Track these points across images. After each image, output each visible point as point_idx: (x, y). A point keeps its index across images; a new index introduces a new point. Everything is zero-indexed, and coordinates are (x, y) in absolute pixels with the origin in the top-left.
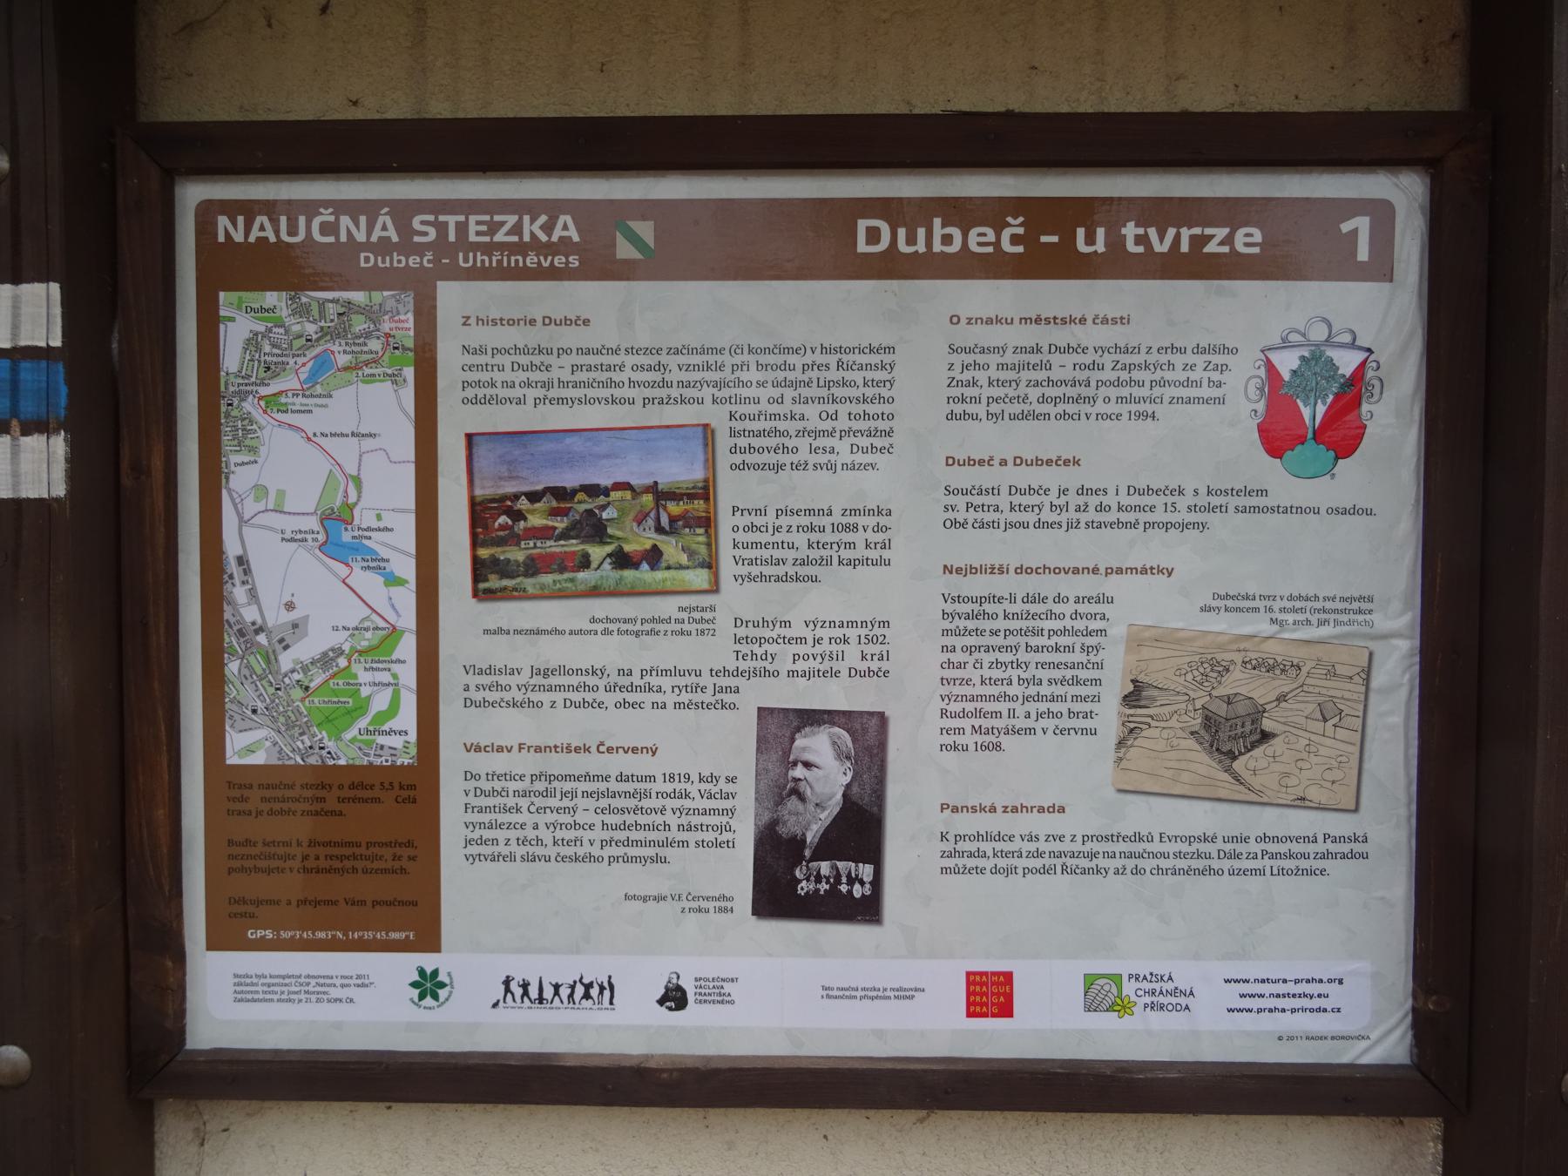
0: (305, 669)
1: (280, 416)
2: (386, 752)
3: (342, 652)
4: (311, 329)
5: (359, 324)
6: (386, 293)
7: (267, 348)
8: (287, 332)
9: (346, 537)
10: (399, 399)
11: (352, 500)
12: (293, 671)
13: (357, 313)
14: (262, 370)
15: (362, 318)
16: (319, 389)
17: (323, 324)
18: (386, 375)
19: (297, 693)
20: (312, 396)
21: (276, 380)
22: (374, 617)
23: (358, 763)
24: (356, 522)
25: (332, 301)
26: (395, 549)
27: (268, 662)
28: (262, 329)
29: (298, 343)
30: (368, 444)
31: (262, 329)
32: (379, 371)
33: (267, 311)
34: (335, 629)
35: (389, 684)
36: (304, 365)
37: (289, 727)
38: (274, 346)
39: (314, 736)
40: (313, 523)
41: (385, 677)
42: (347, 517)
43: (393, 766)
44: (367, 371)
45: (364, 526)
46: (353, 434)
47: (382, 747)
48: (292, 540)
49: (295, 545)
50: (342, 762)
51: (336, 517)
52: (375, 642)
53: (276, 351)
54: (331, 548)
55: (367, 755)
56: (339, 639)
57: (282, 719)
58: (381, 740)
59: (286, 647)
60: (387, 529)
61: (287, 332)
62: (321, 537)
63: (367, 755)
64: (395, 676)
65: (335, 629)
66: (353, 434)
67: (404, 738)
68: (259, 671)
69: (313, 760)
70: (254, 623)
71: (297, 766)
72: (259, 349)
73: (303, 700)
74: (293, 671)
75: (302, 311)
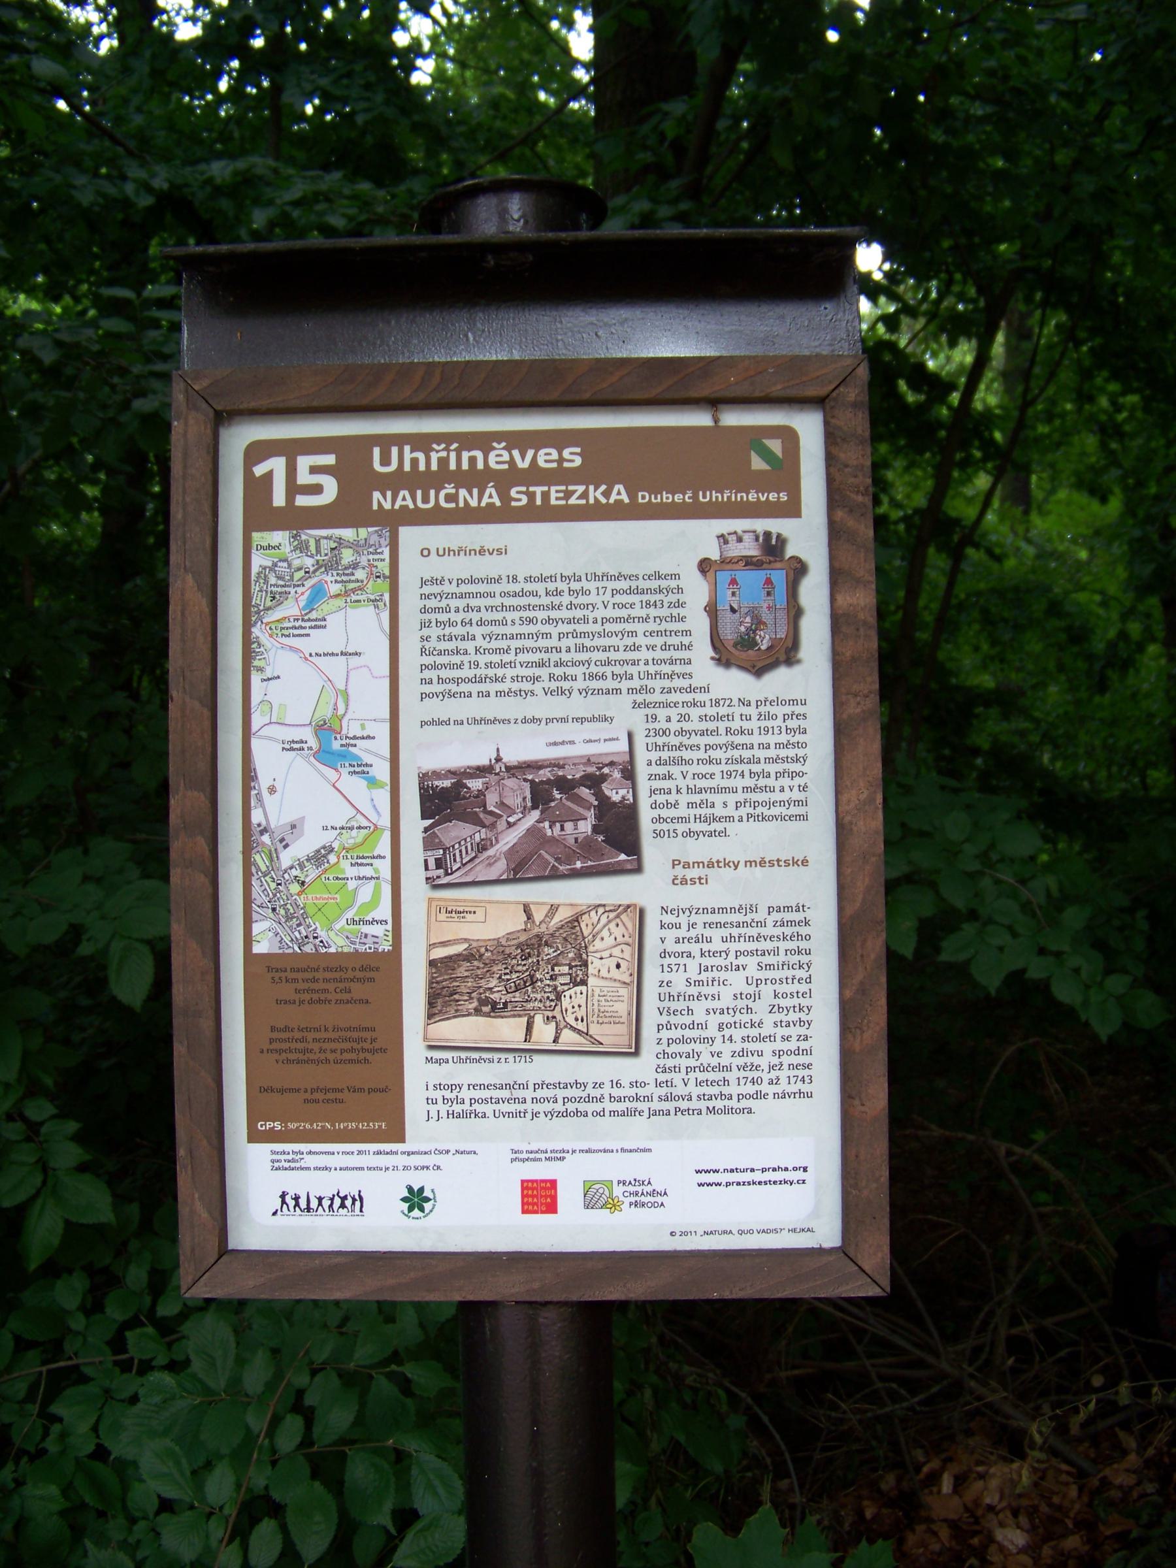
0: (302, 866)
1: (284, 640)
2: (370, 940)
3: (332, 850)
4: (309, 562)
5: (347, 556)
6: (370, 529)
7: (273, 580)
8: (290, 566)
9: (336, 745)
10: (379, 620)
11: (341, 712)
12: (291, 868)
13: (347, 547)
14: (269, 599)
15: (350, 551)
16: (314, 615)
17: (318, 558)
18: (369, 600)
19: (295, 888)
20: (309, 620)
21: (279, 608)
22: (359, 816)
23: (346, 950)
24: (344, 732)
25: (326, 538)
26: (376, 755)
27: (271, 860)
28: (270, 564)
29: (298, 575)
30: (354, 661)
31: (270, 564)
32: (364, 597)
33: (274, 548)
34: (325, 828)
35: (372, 878)
36: (303, 594)
37: (289, 918)
38: (279, 578)
39: (309, 926)
40: (308, 735)
41: (367, 871)
42: (337, 727)
43: (376, 952)
44: (354, 598)
45: (351, 735)
46: (342, 653)
47: (366, 936)
48: (292, 749)
49: (293, 753)
50: (332, 950)
51: (323, 728)
52: (359, 840)
53: (281, 583)
54: (325, 756)
55: (353, 943)
56: (328, 837)
57: (282, 912)
58: (366, 929)
59: (286, 846)
60: (369, 737)
61: (290, 566)
62: (315, 746)
63: (353, 943)
64: (376, 871)
65: (325, 828)
66: (342, 653)
67: (384, 927)
68: (264, 869)
69: (308, 949)
70: (259, 825)
71: (295, 953)
72: (266, 581)
73: (299, 894)
74: (291, 868)
75: (302, 548)
